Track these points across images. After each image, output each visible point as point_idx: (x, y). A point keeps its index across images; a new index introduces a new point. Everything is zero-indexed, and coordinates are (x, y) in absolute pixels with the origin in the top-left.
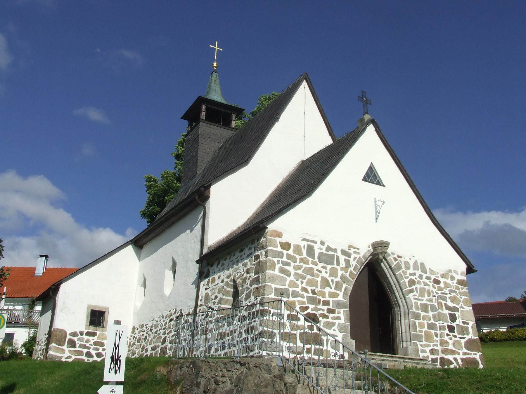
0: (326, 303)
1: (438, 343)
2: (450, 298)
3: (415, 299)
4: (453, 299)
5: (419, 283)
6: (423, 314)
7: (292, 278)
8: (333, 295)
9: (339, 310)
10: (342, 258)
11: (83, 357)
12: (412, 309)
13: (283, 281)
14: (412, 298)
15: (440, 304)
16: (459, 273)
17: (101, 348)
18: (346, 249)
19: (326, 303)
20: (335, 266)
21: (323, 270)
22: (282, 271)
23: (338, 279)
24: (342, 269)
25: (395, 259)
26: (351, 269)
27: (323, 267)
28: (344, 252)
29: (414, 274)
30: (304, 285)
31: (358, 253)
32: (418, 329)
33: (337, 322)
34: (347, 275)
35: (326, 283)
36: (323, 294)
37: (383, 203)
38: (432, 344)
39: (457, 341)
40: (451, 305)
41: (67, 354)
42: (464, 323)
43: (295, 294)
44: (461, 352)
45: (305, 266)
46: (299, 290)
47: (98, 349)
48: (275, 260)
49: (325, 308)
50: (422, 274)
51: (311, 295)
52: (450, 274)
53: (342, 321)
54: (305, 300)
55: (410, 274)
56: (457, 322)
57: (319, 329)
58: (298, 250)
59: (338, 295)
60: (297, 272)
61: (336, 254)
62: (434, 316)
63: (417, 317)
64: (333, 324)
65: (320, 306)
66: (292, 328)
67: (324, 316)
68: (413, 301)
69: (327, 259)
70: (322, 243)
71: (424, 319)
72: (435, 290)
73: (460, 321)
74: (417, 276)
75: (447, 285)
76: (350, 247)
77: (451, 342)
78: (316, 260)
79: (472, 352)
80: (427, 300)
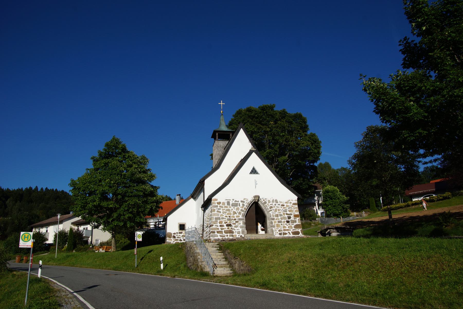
4: (289, 211)
5: (274, 207)
6: (276, 218)
7: (222, 213)
8: (237, 217)
11: (179, 241)
13: (218, 215)
18: (243, 200)
19: (235, 219)
22: (218, 211)
23: (240, 211)
25: (264, 200)
26: (245, 207)
28: (242, 201)
34: (243, 209)
35: (235, 213)
36: (234, 217)
40: (288, 213)
43: (222, 218)
46: (224, 217)
48: (215, 208)
49: (235, 221)
53: (241, 225)
56: (291, 219)
57: (231, 228)
58: (224, 203)
62: (281, 218)
63: (273, 219)
65: (233, 221)
66: (222, 229)
67: (234, 224)
69: (235, 205)
76: (244, 199)
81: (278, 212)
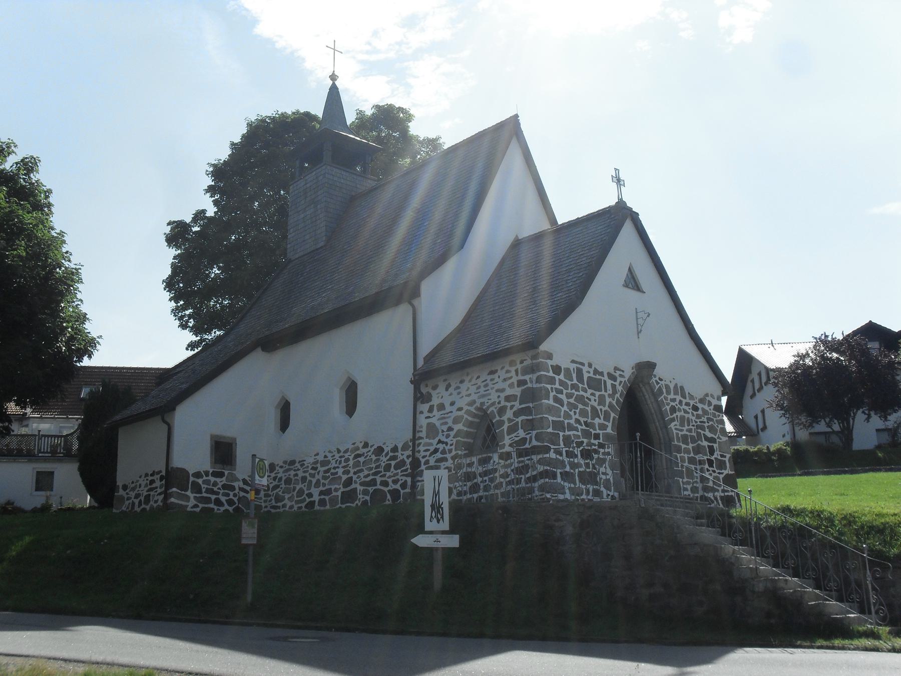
0: (597, 436)
1: (698, 480)
2: (708, 427)
5: (680, 410)
6: (684, 446)
8: (603, 427)
11: (212, 506)
14: (673, 428)
15: (699, 434)
17: (231, 494)
18: (612, 372)
19: (597, 436)
20: (603, 393)
21: (592, 398)
24: (609, 395)
26: (618, 395)
28: (611, 376)
29: (674, 400)
30: (577, 416)
34: (614, 402)
37: (648, 316)
40: (709, 435)
41: (192, 502)
43: (570, 427)
44: (720, 489)
45: (576, 393)
46: (572, 421)
47: (228, 495)
48: (549, 386)
49: (596, 442)
51: (584, 427)
54: (580, 433)
64: (604, 461)
68: (675, 431)
70: (590, 365)
74: (677, 402)
75: (705, 412)
76: (616, 369)
78: (586, 386)
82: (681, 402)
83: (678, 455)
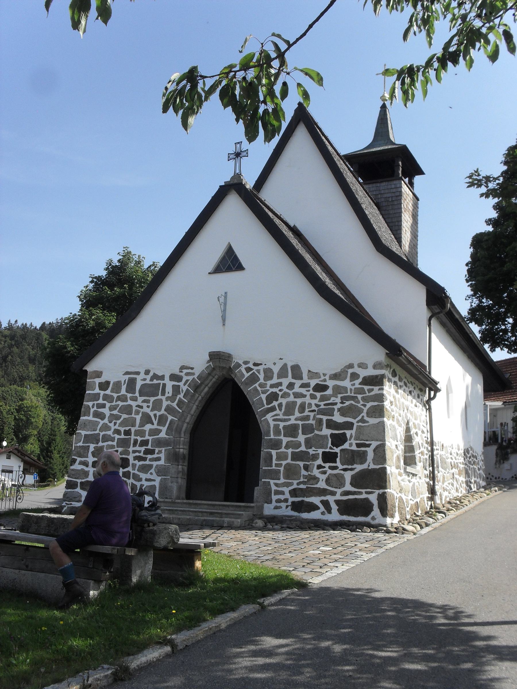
2: (339, 410)
3: (274, 420)
5: (285, 395)
6: (285, 440)
7: (106, 421)
9: (160, 449)
10: (170, 385)
12: (268, 434)
14: (270, 421)
15: (320, 422)
16: (370, 366)
18: (177, 372)
19: (145, 443)
20: (160, 397)
21: (145, 405)
22: (97, 415)
24: (168, 399)
25: (248, 370)
26: (181, 396)
27: (144, 401)
30: (117, 427)
31: (193, 374)
32: (274, 462)
33: (155, 464)
34: (174, 405)
35: (147, 419)
36: (141, 433)
38: (295, 482)
39: (335, 475)
40: (338, 418)
42: (358, 445)
45: (121, 404)
48: (90, 404)
49: (143, 449)
50: (293, 381)
52: (350, 371)
53: (162, 462)
55: (272, 386)
56: (346, 446)
58: (117, 386)
59: (160, 431)
60: (112, 412)
61: (162, 382)
63: (276, 445)
64: (151, 466)
68: (272, 423)
71: (287, 447)
72: (314, 402)
73: (351, 445)
74: (284, 387)
75: (337, 390)
76: (182, 368)
77: (323, 477)
78: (137, 394)
79: (363, 491)
80: (296, 419)
81: (297, 414)
82: (291, 386)
83: (274, 452)
